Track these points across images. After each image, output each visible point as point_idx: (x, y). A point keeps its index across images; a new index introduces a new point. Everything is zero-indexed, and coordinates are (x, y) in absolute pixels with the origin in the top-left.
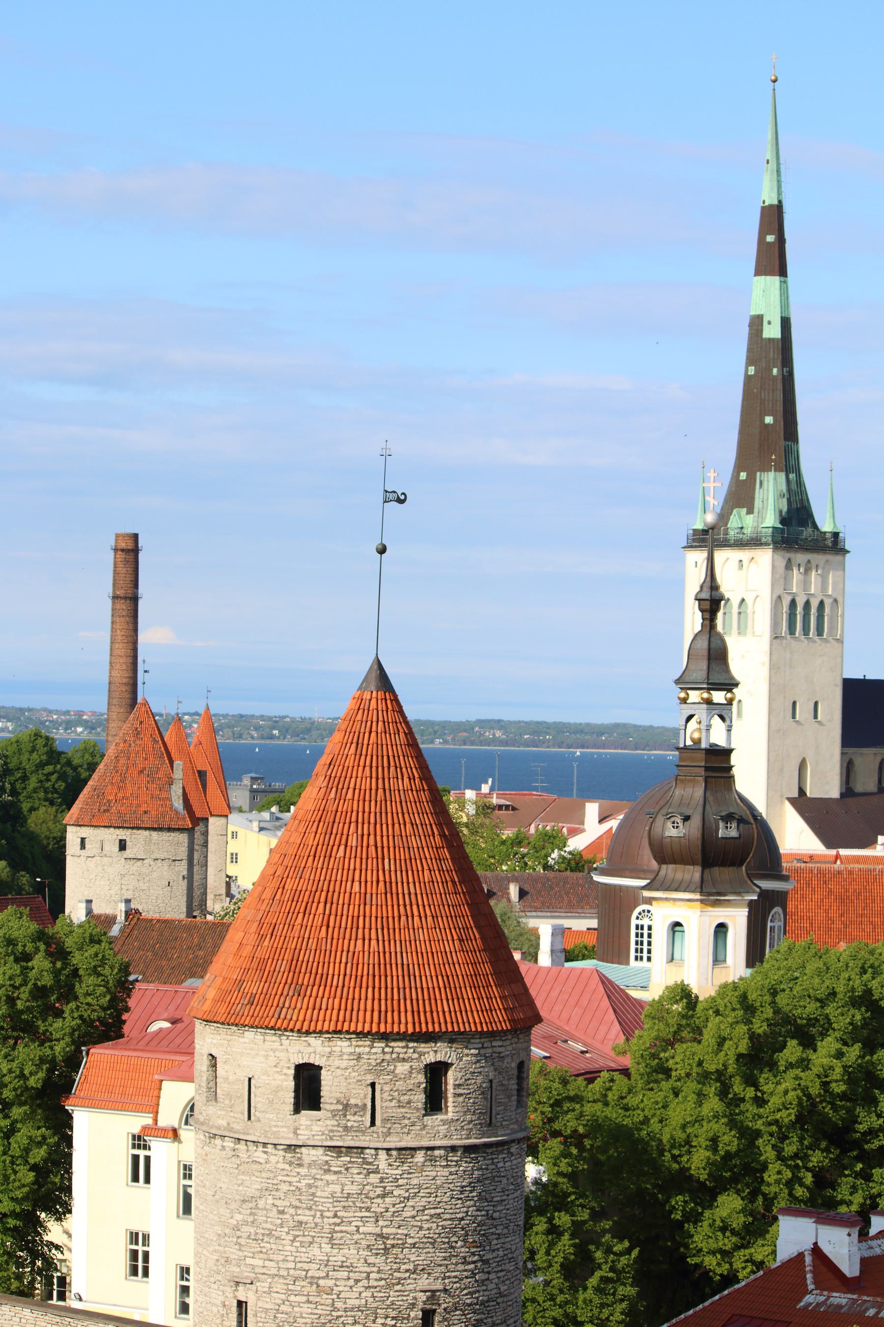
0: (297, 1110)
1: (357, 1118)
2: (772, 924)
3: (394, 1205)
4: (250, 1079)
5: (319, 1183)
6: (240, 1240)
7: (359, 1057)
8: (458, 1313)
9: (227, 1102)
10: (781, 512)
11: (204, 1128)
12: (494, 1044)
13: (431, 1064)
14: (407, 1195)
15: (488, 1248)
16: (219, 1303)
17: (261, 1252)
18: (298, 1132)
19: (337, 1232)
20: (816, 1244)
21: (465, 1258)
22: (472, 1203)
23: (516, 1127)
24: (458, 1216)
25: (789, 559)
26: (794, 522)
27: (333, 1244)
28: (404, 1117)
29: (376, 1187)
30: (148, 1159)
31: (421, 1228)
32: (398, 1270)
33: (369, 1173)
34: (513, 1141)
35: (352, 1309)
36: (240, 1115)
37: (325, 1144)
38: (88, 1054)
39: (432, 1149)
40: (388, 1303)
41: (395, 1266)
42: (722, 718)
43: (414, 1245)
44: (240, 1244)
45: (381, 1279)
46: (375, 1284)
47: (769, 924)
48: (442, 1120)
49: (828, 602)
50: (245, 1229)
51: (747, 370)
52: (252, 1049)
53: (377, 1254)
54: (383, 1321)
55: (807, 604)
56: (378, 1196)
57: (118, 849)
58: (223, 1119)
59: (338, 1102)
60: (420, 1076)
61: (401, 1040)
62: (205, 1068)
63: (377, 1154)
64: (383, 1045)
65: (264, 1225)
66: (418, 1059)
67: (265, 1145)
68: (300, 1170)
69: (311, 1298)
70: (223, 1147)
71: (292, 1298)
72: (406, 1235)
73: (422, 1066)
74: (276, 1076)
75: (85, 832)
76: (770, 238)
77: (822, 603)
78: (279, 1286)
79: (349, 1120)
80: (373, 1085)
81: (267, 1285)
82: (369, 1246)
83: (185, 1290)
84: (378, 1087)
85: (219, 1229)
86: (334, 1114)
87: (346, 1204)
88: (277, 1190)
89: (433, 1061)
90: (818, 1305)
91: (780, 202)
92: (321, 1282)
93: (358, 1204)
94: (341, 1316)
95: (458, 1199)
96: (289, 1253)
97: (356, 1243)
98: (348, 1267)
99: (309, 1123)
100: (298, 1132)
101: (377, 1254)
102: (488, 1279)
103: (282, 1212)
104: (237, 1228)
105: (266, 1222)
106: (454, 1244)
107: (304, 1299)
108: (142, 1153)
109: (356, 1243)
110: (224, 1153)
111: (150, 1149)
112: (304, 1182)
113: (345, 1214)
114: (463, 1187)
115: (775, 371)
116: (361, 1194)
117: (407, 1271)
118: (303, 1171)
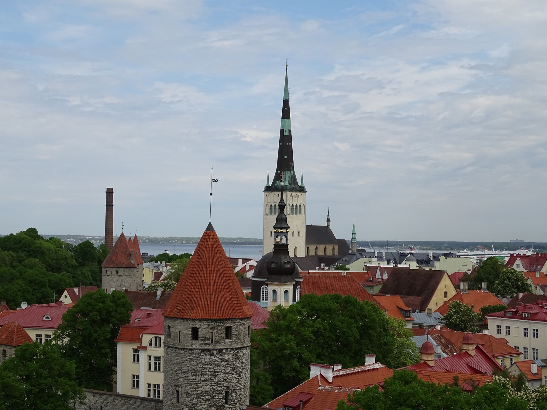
0: (192, 340)
1: (208, 341)
2: (298, 290)
3: (218, 364)
4: (179, 332)
5: (198, 358)
6: (177, 374)
7: (208, 325)
8: (235, 392)
9: (173, 338)
10: (289, 181)
11: (167, 345)
12: (243, 321)
13: (227, 327)
14: (221, 361)
15: (241, 375)
16: (171, 391)
17: (183, 377)
18: (193, 345)
19: (203, 371)
20: (321, 373)
21: (236, 377)
22: (238, 363)
23: (248, 343)
24: (234, 366)
25: (291, 194)
26: (293, 184)
27: (202, 375)
28: (220, 341)
29: (213, 359)
30: (138, 356)
31: (225, 370)
32: (219, 381)
33: (211, 355)
34: (247, 347)
35: (207, 392)
36: (177, 341)
37: (200, 348)
38: (121, 327)
39: (227, 349)
40: (216, 390)
41: (218, 380)
42: (286, 237)
43: (223, 374)
44: (177, 375)
45: (214, 384)
46: (213, 385)
47: (297, 290)
48: (230, 341)
49: (302, 205)
50: (178, 371)
51: (280, 144)
52: (180, 324)
53: (213, 377)
54: (215, 395)
55: (296, 205)
56: (214, 362)
57: (116, 273)
58: (172, 342)
59: (203, 337)
60: (224, 330)
61: (219, 321)
62: (167, 329)
63: (213, 351)
64: (214, 322)
65: (183, 370)
66: (224, 326)
67: (184, 349)
68: (193, 355)
69: (196, 389)
70: (173, 350)
71: (191, 389)
72: (221, 372)
73: (225, 327)
74: (187, 331)
75: (107, 269)
76: (286, 109)
77: (300, 205)
78: (188, 386)
79: (206, 342)
80: (212, 333)
81: (184, 386)
82: (211, 375)
83: (149, 390)
84: (213, 333)
85: (171, 372)
86: (202, 340)
87: (205, 364)
88: (187, 361)
89: (227, 326)
90: (323, 389)
91: (288, 99)
92: (199, 385)
93: (208, 364)
94: (204, 394)
95: (234, 362)
96: (190, 377)
97: (208, 374)
98: (206, 381)
99: (195, 343)
100: (193, 345)
101: (213, 377)
102: (242, 383)
103: (188, 367)
104: (176, 371)
105: (184, 369)
106: (233, 374)
107: (194, 389)
108: (136, 354)
109: (208, 374)
110: (172, 351)
111: (139, 353)
112: (194, 359)
113: (205, 367)
114: (235, 359)
115: (287, 144)
116: (209, 361)
117: (221, 381)
118: (194, 355)
